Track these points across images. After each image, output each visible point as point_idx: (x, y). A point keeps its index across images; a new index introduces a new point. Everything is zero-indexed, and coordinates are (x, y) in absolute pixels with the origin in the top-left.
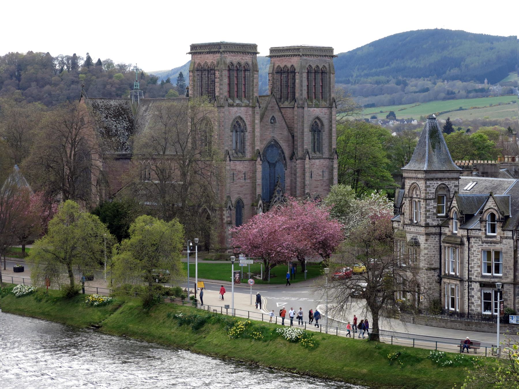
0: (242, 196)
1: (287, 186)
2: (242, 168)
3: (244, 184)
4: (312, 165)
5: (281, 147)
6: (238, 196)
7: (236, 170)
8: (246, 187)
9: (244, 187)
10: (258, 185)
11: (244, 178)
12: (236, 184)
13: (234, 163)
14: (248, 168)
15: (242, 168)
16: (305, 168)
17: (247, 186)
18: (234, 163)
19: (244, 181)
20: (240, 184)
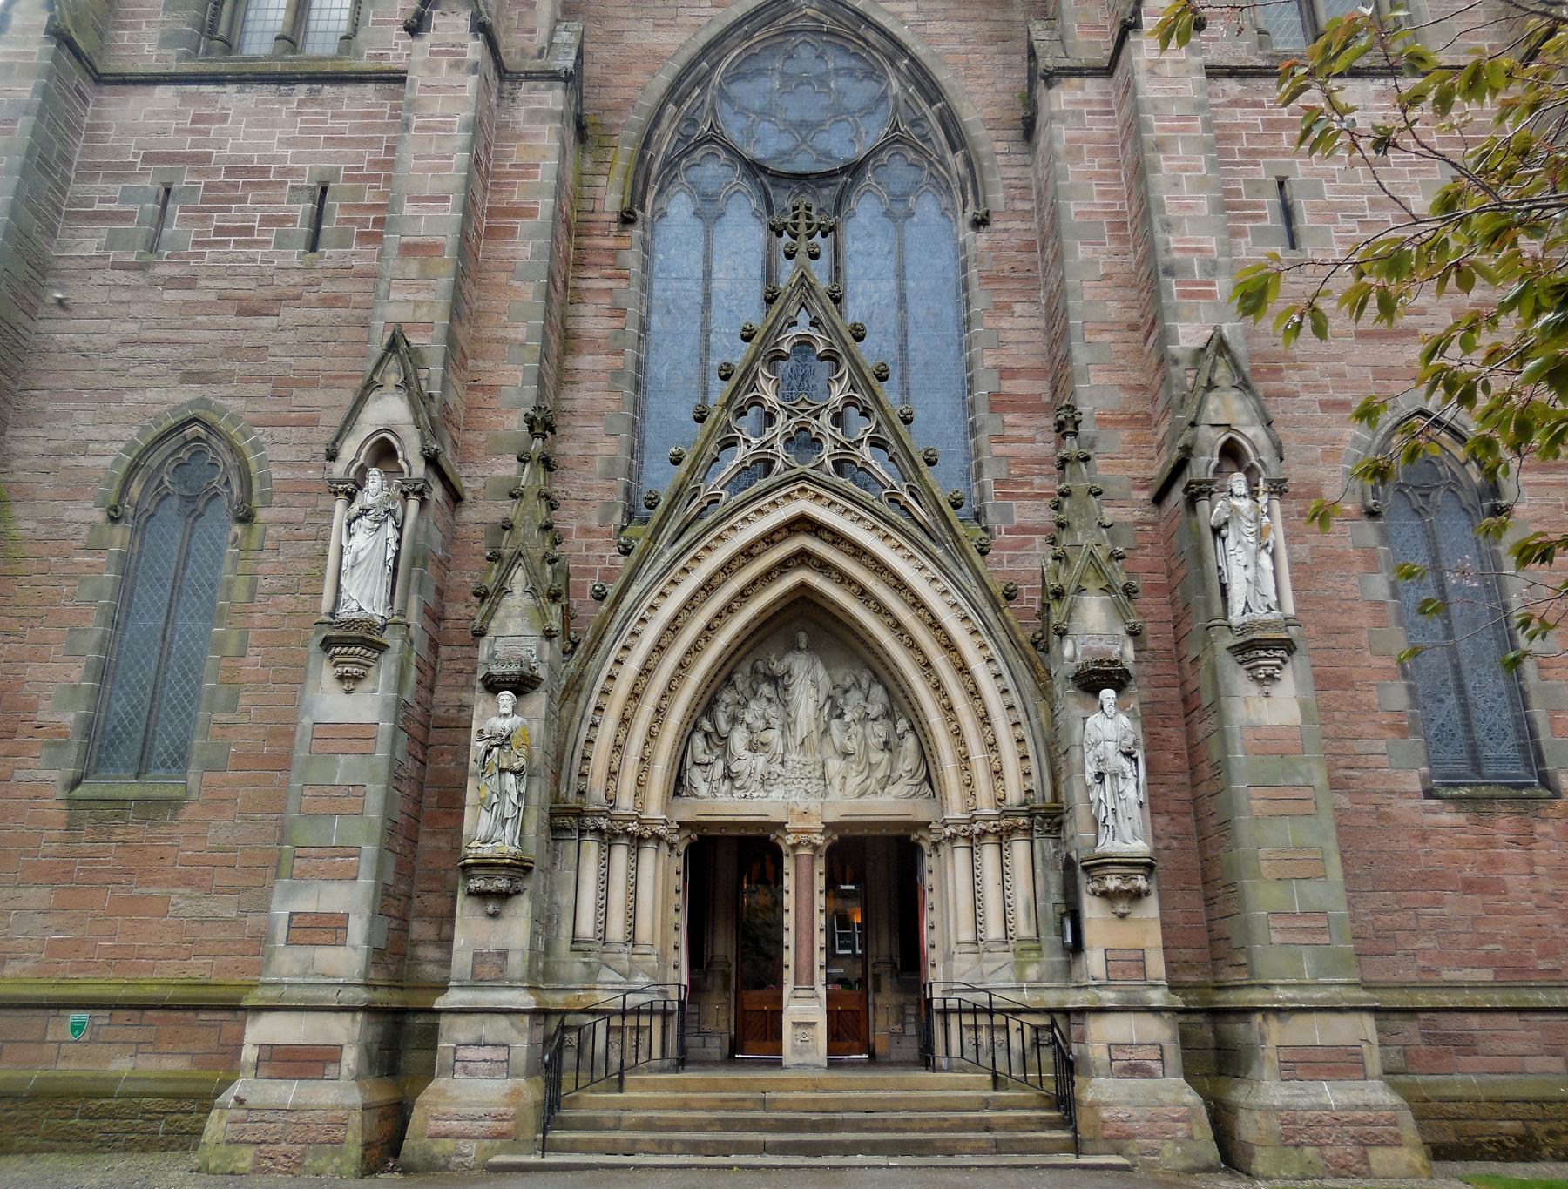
0: (228, 401)
1: (1006, 373)
2: (290, 142)
3: (284, 283)
4: (1270, 124)
5: (901, 48)
6: (185, 395)
7: (207, 158)
8: (320, 313)
9: (289, 315)
10: (408, 250)
11: (302, 229)
12: (171, 283)
13: (186, 99)
14: (369, 142)
15: (290, 142)
16: (1137, 110)
17: (329, 302)
18: (186, 99)
19: (294, 256)
20: (245, 288)
